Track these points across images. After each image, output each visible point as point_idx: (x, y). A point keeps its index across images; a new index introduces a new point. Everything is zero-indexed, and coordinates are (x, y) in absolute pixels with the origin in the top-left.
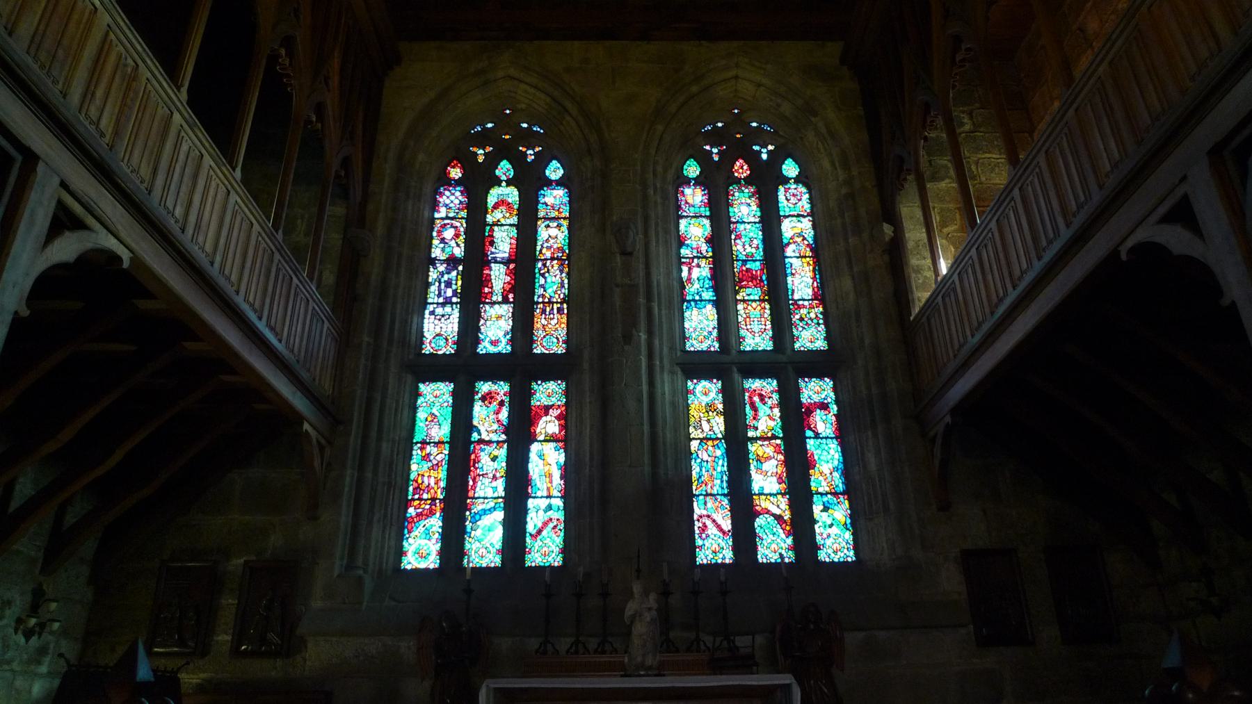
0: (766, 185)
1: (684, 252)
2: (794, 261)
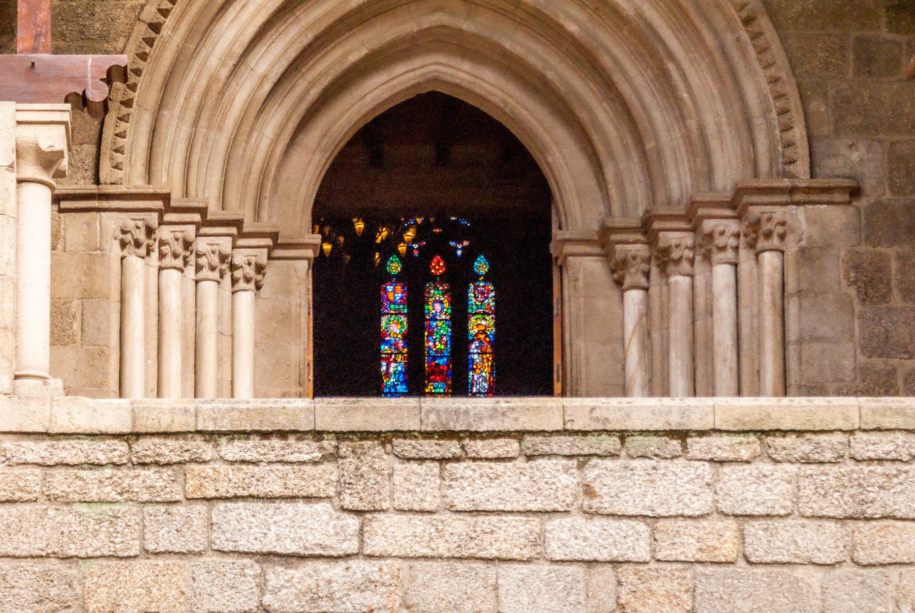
0: (458, 282)
1: (384, 348)
2: (476, 357)
